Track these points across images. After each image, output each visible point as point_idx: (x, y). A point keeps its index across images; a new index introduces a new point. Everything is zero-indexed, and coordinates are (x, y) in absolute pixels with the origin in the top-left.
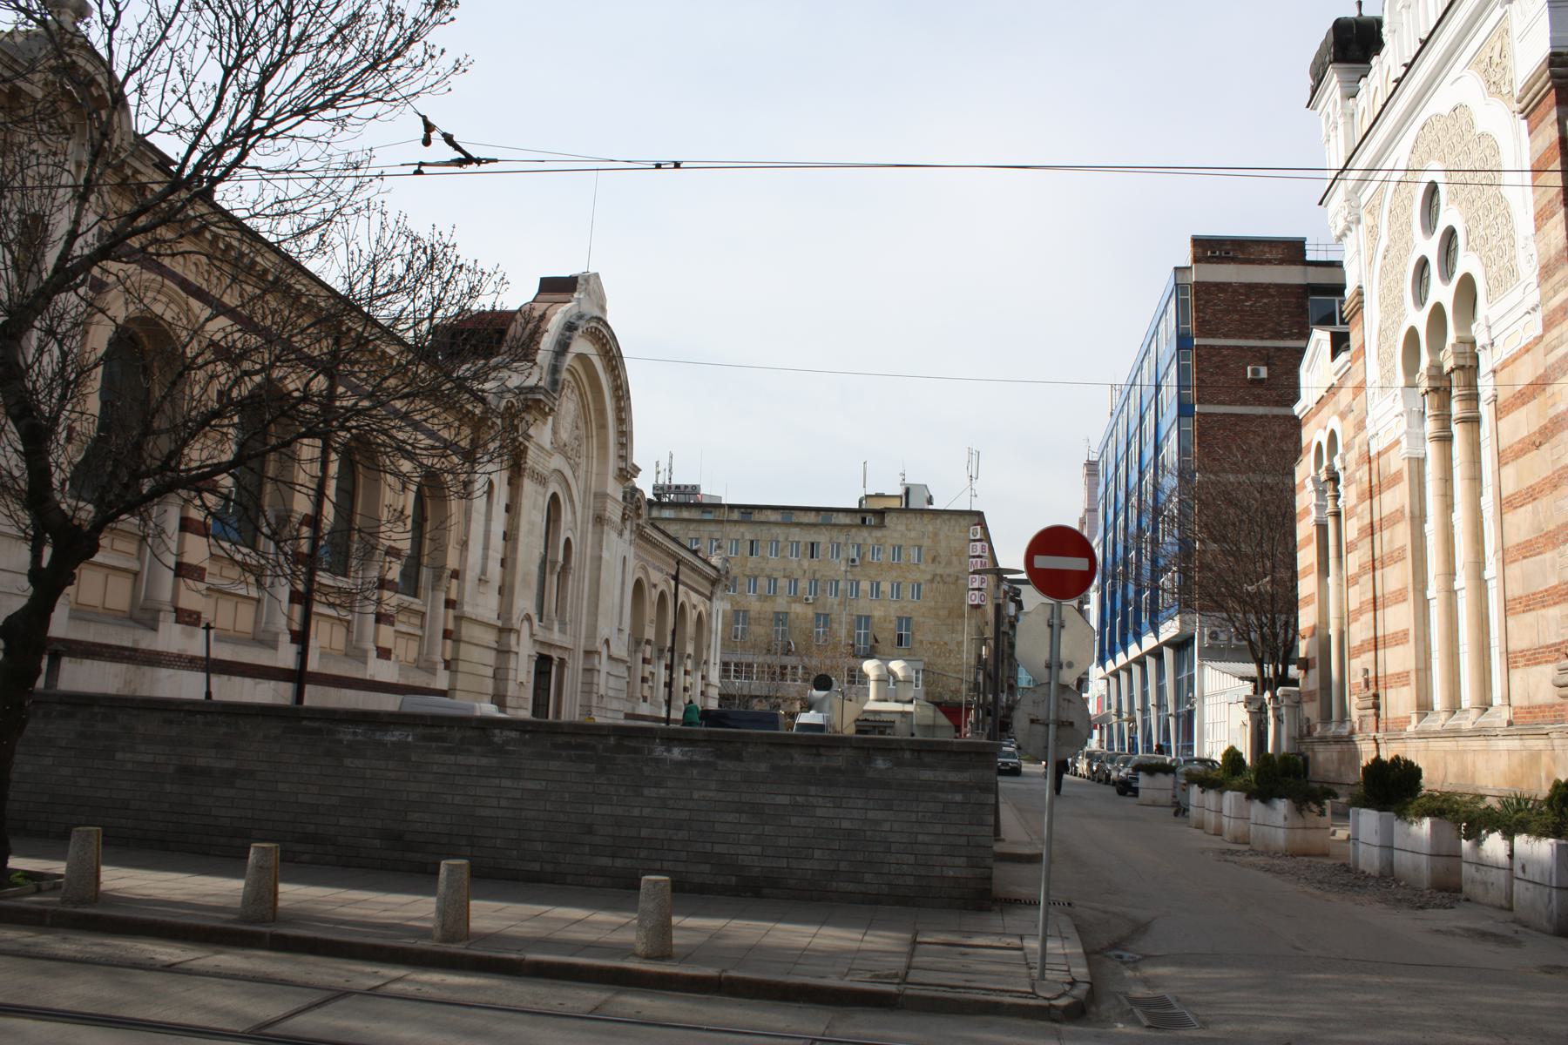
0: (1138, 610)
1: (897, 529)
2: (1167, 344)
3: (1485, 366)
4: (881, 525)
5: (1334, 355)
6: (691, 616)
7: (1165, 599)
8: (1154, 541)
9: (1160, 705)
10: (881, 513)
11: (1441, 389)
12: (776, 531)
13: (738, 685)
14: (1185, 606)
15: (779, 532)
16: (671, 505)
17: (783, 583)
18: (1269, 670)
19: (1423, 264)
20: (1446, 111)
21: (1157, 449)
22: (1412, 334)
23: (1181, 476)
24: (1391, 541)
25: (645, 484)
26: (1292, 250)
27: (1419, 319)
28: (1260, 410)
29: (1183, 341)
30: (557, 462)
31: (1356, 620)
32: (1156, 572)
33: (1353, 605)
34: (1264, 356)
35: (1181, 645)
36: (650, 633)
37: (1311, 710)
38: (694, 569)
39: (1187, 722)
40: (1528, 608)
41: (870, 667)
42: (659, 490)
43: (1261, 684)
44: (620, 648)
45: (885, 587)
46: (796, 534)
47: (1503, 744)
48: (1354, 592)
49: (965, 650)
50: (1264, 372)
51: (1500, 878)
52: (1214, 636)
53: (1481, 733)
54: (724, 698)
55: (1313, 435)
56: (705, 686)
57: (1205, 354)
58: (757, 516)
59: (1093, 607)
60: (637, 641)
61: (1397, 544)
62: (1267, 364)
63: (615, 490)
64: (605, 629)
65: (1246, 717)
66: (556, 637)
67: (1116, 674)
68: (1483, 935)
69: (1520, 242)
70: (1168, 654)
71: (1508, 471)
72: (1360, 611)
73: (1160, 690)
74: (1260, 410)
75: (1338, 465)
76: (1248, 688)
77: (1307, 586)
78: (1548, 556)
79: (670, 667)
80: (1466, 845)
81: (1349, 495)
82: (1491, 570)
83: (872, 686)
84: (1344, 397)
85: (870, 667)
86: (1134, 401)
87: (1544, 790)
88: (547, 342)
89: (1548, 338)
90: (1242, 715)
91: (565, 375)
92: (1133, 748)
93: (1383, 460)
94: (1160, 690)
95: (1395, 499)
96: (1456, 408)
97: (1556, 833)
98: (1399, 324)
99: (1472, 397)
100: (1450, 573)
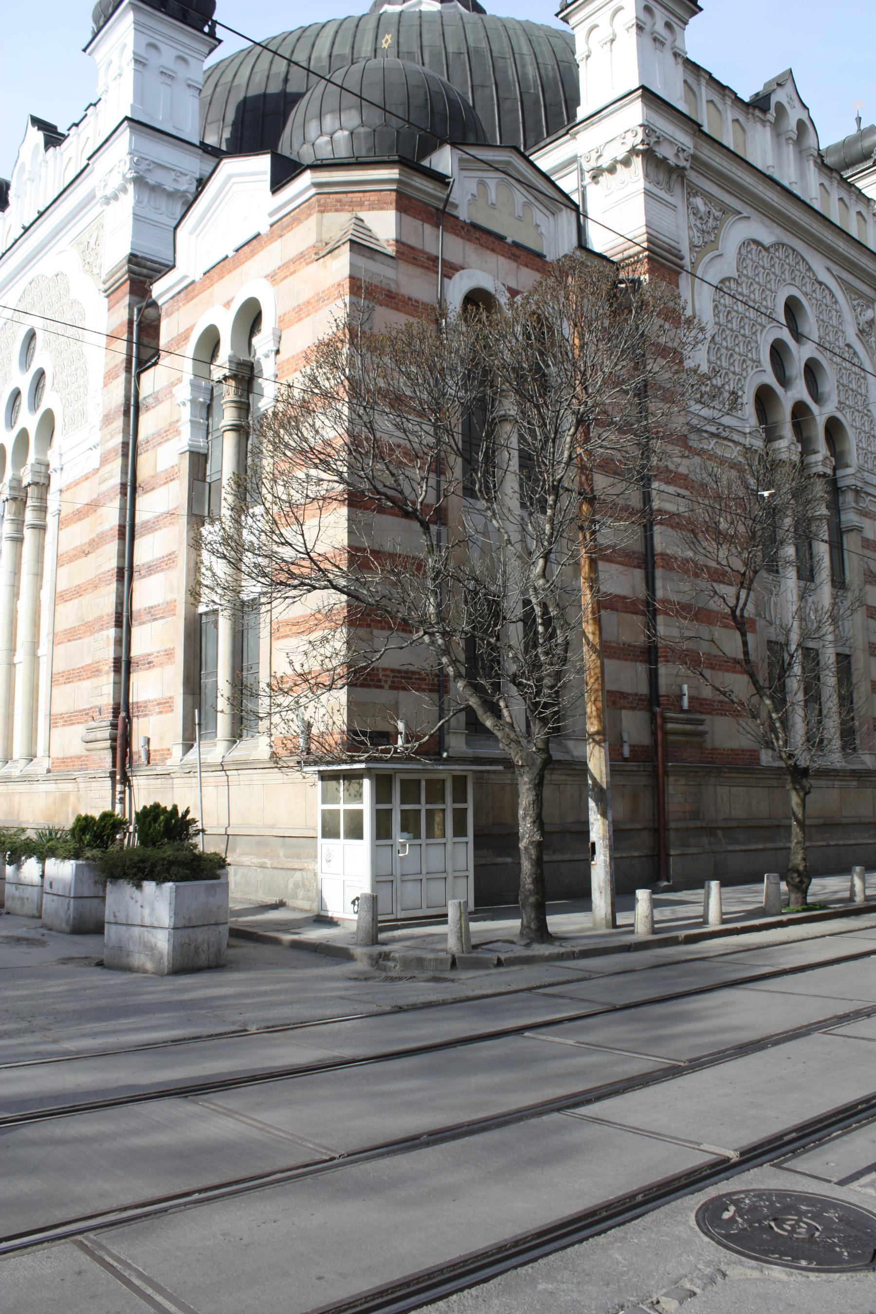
40: (68, 681)
47: (42, 787)
51: (33, 893)
53: (26, 779)
68: (19, 940)
71: (63, 571)
78: (86, 640)
80: (9, 870)
82: (43, 650)
87: (69, 823)
89: (104, 470)
97: (76, 856)
99: (42, 509)
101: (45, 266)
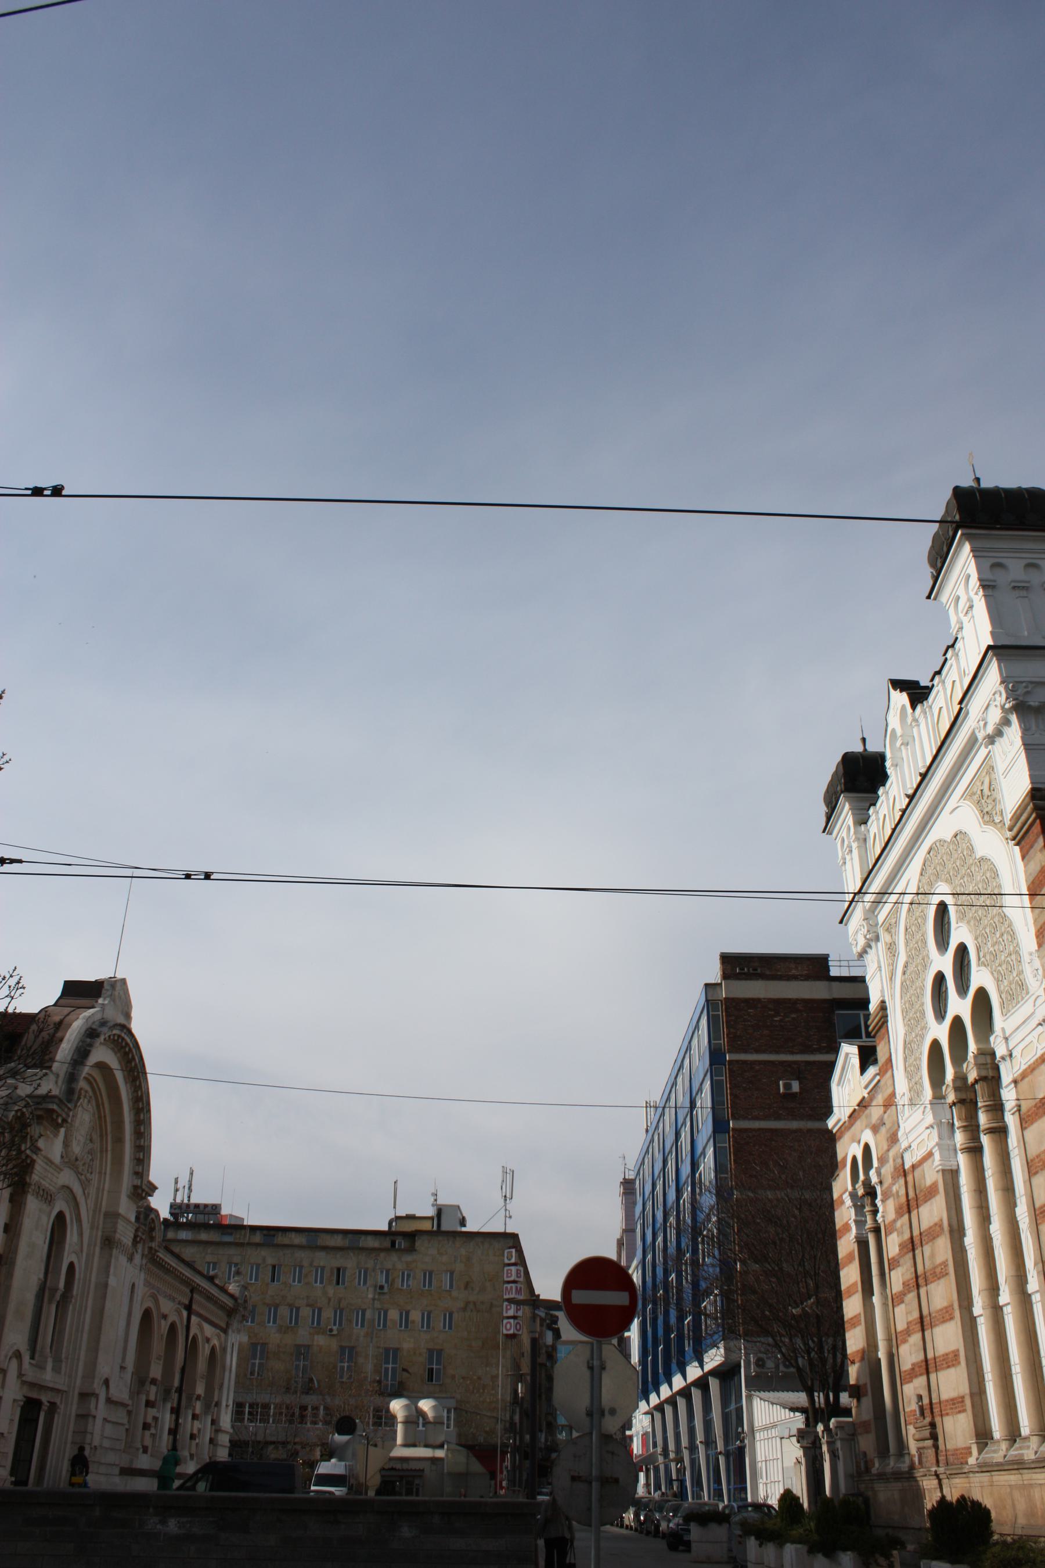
0: (680, 1337)
1: (428, 1253)
2: (700, 1060)
3: (1006, 1078)
4: (411, 1249)
5: (863, 1069)
6: (204, 1351)
7: (708, 1325)
8: (695, 1263)
9: (709, 1442)
10: (412, 1236)
11: (967, 1102)
12: (300, 1254)
13: (253, 1429)
14: (729, 1333)
15: (301, 1255)
16: (190, 1226)
17: (306, 1312)
18: (820, 1398)
19: (940, 978)
20: (948, 836)
21: (694, 1166)
22: (935, 1045)
23: (718, 1194)
24: (933, 1256)
25: (161, 1204)
26: (816, 966)
27: (941, 1032)
28: (794, 1125)
29: (716, 1056)
30: (66, 1177)
31: (905, 1341)
32: (698, 1295)
33: (901, 1326)
34: (795, 1071)
35: (727, 1373)
36: (156, 1371)
37: (867, 1443)
38: (210, 1298)
39: (738, 1459)
41: (397, 1406)
42: (177, 1209)
43: (813, 1415)
44: (120, 1391)
45: (415, 1316)
46: (322, 1259)
48: (900, 1311)
49: (500, 1385)
50: (796, 1087)
52: (760, 1363)
54: (235, 1445)
55: (849, 1150)
56: (213, 1433)
57: (737, 1070)
58: (280, 1239)
59: (634, 1333)
60: (141, 1380)
61: (939, 1259)
62: (798, 1078)
63: (127, 1209)
64: (105, 1368)
65: (800, 1453)
66: (48, 1376)
67: (660, 1408)
69: (1026, 958)
70: (714, 1384)
72: (908, 1332)
73: (708, 1425)
74: (794, 1125)
75: (874, 1179)
76: (798, 1421)
77: (852, 1307)
79: (176, 1411)
81: (887, 1210)
83: (400, 1428)
84: (875, 1112)
85: (397, 1406)
86: (669, 1117)
88: (65, 1050)
90: (794, 1451)
91: (82, 1084)
92: (682, 1494)
93: (917, 1172)
94: (708, 1425)
95: (933, 1212)
96: (983, 1119)
98: (923, 1037)
99: (997, 1108)
100: (993, 1289)
101: (942, 829)
